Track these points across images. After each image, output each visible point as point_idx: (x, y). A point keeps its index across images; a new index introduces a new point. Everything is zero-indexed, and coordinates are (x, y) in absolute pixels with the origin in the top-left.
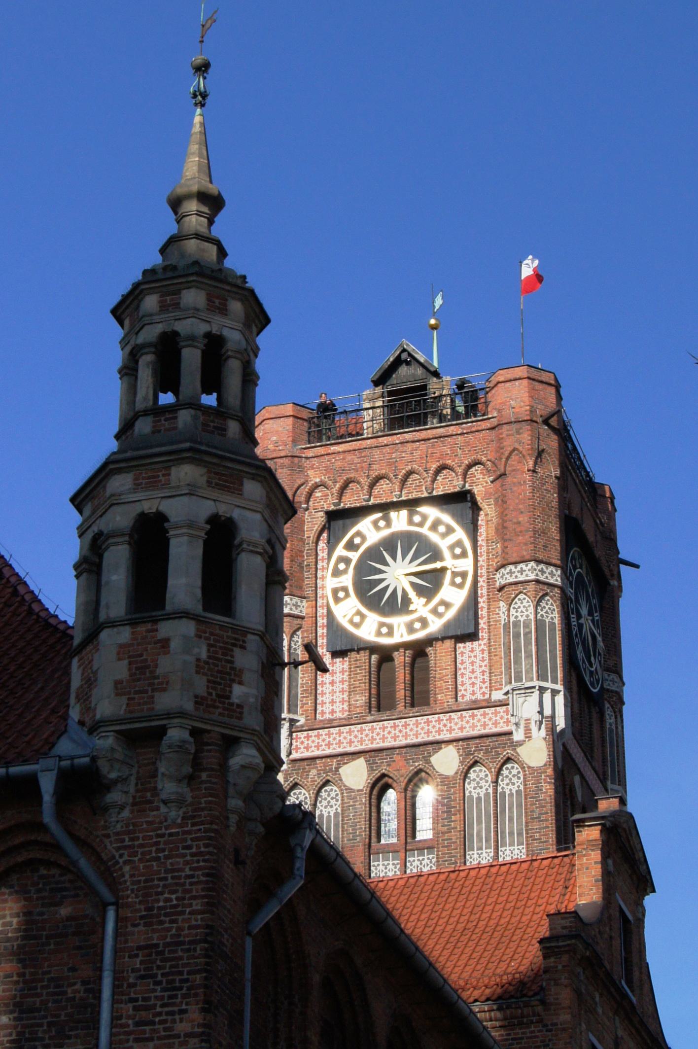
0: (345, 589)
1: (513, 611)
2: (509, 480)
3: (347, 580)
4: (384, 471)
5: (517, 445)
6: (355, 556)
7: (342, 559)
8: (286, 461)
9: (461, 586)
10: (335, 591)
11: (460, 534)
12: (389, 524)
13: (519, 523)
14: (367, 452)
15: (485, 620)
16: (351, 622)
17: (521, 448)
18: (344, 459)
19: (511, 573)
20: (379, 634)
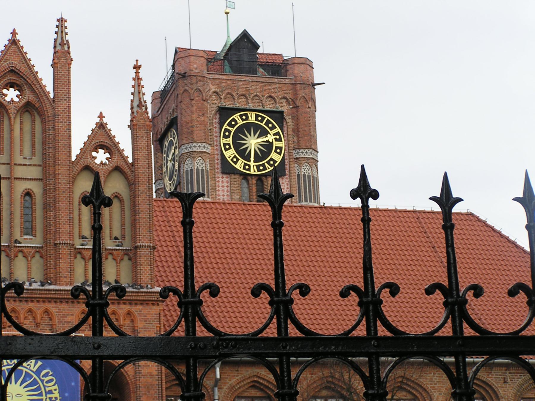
0: (229, 144)
1: (303, 170)
2: (301, 110)
3: (230, 140)
4: (244, 93)
5: (303, 95)
6: (233, 130)
7: (226, 130)
8: (202, 78)
9: (280, 154)
10: (225, 145)
11: (278, 129)
12: (247, 119)
13: (305, 130)
14: (236, 82)
15: (288, 170)
16: (232, 160)
17: (306, 96)
18: (226, 82)
19: (302, 153)
20: (244, 168)
